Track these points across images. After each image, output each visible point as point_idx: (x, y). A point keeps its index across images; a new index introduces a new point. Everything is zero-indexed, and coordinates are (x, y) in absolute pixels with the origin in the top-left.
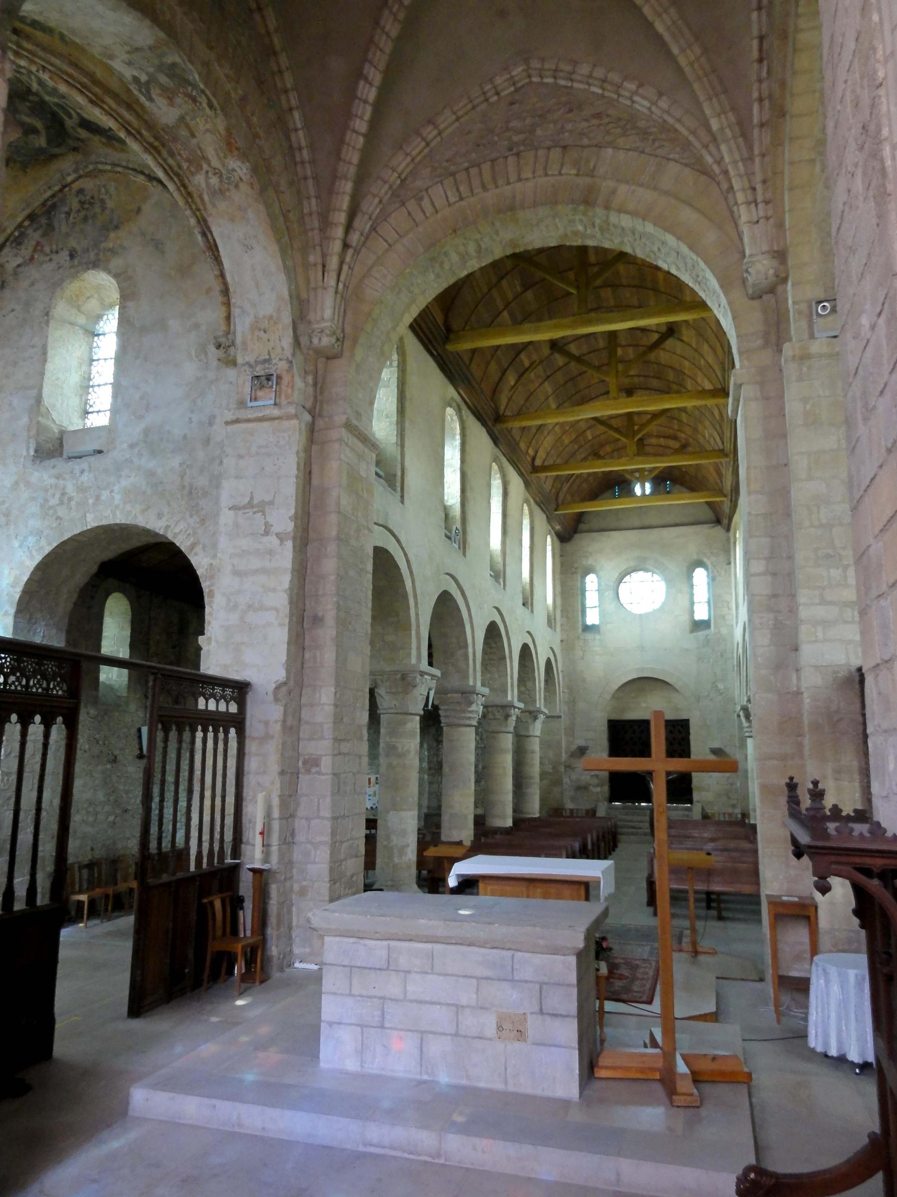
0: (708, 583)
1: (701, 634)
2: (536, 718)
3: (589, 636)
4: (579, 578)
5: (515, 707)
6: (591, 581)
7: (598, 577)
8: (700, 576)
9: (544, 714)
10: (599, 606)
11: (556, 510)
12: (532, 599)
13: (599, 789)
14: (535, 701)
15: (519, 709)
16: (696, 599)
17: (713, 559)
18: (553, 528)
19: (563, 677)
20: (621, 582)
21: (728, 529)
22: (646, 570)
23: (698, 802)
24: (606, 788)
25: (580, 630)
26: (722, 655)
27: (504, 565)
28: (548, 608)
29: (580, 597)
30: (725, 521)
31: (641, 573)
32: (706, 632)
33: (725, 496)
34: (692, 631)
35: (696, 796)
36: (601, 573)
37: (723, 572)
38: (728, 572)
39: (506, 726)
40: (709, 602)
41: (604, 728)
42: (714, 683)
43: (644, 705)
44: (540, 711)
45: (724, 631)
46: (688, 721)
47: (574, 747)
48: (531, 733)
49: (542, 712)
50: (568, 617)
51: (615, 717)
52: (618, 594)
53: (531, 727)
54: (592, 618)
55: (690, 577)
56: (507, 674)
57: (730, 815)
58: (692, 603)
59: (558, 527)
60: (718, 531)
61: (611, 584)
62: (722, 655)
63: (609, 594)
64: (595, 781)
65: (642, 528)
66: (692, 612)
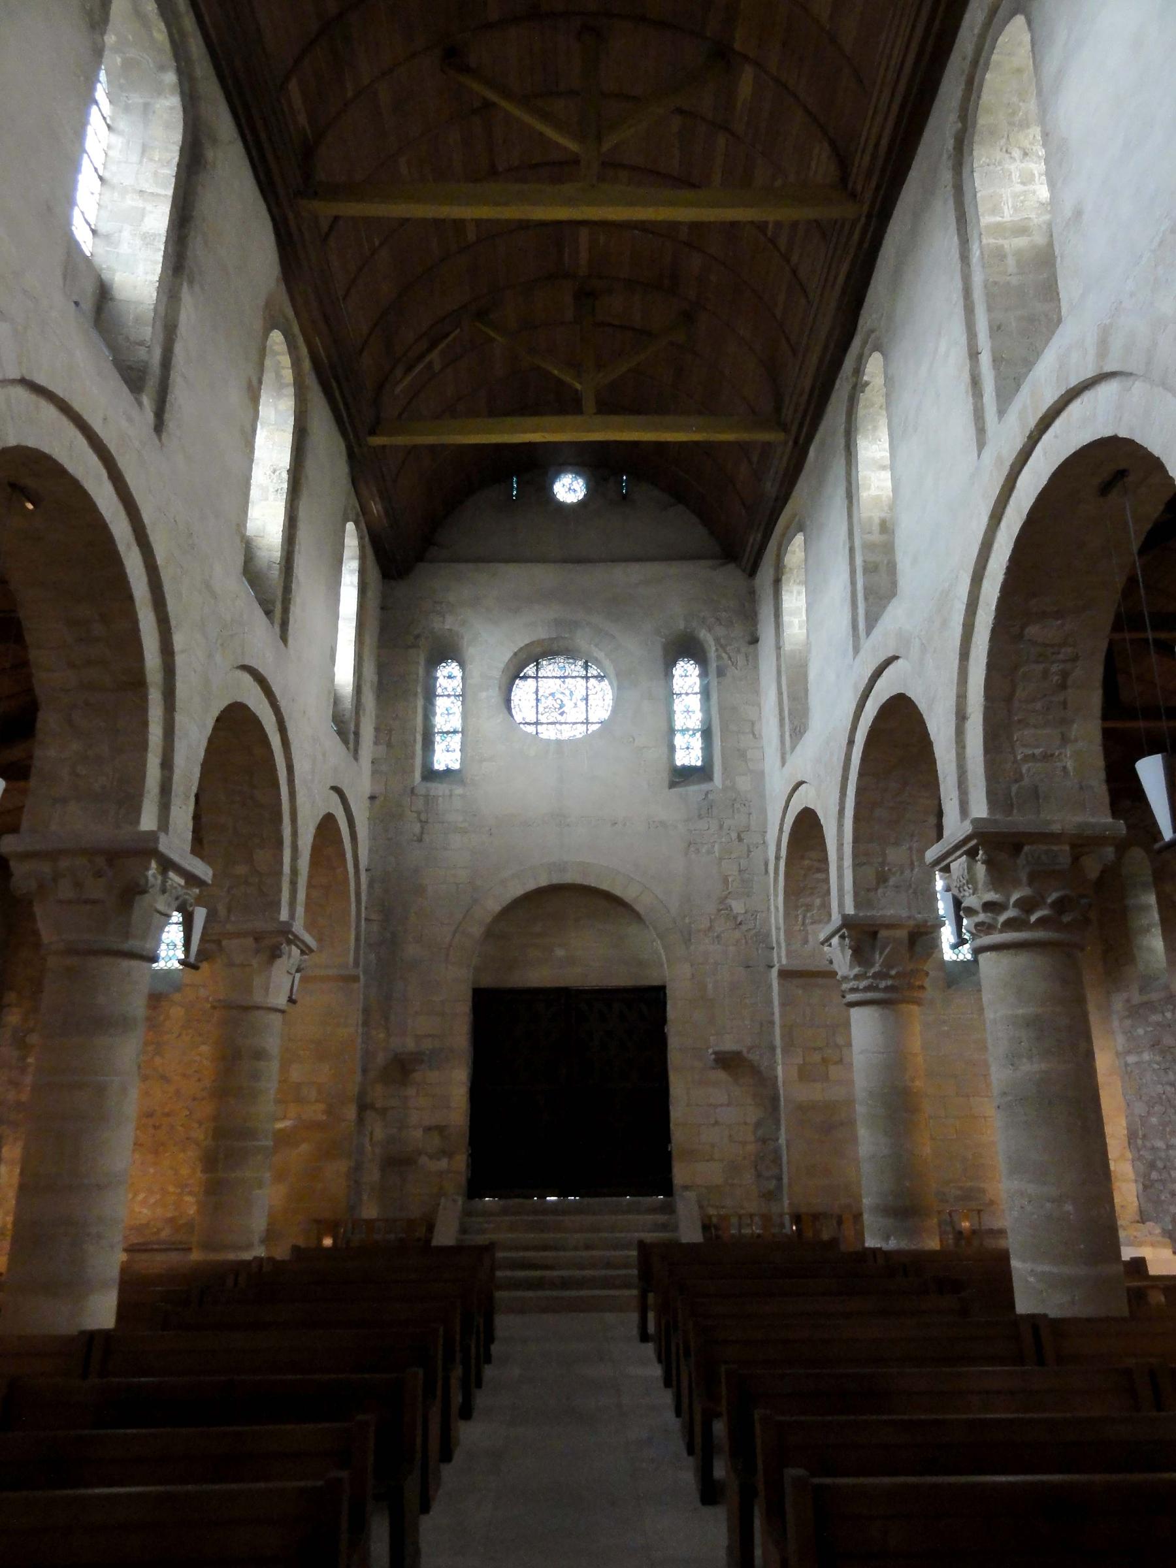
0: (705, 693)
1: (694, 790)
2: (274, 954)
3: (439, 789)
4: (422, 662)
5: (167, 865)
6: (448, 676)
7: (462, 665)
8: (686, 675)
9: (306, 950)
10: (462, 732)
11: (372, 432)
12: (286, 610)
13: (443, 1164)
14: (277, 905)
15: (192, 879)
16: (679, 722)
17: (720, 631)
18: (364, 510)
19: (371, 885)
20: (517, 676)
21: (752, 571)
22: (570, 653)
23: (686, 1188)
24: (461, 1161)
25: (418, 775)
26: (740, 839)
27: (166, 363)
28: (337, 701)
29: (420, 703)
30: (755, 538)
31: (560, 659)
32: (705, 787)
33: (784, 428)
34: (672, 785)
35: (680, 1174)
36: (471, 652)
37: (741, 660)
38: (753, 661)
39: (127, 935)
40: (707, 733)
41: (463, 1009)
42: (723, 900)
43: (560, 952)
44: (285, 933)
45: (744, 784)
46: (662, 989)
47: (381, 1059)
48: (258, 998)
49: (296, 940)
50: (389, 745)
51: (487, 981)
52: (508, 701)
53: (257, 981)
54: (446, 756)
55: (669, 676)
56: (144, 746)
57: (766, 1219)
58: (672, 732)
59: (375, 508)
60: (729, 577)
61: (496, 673)
62: (740, 839)
63: (491, 695)
64: (436, 1141)
65: (565, 561)
66: (672, 749)
